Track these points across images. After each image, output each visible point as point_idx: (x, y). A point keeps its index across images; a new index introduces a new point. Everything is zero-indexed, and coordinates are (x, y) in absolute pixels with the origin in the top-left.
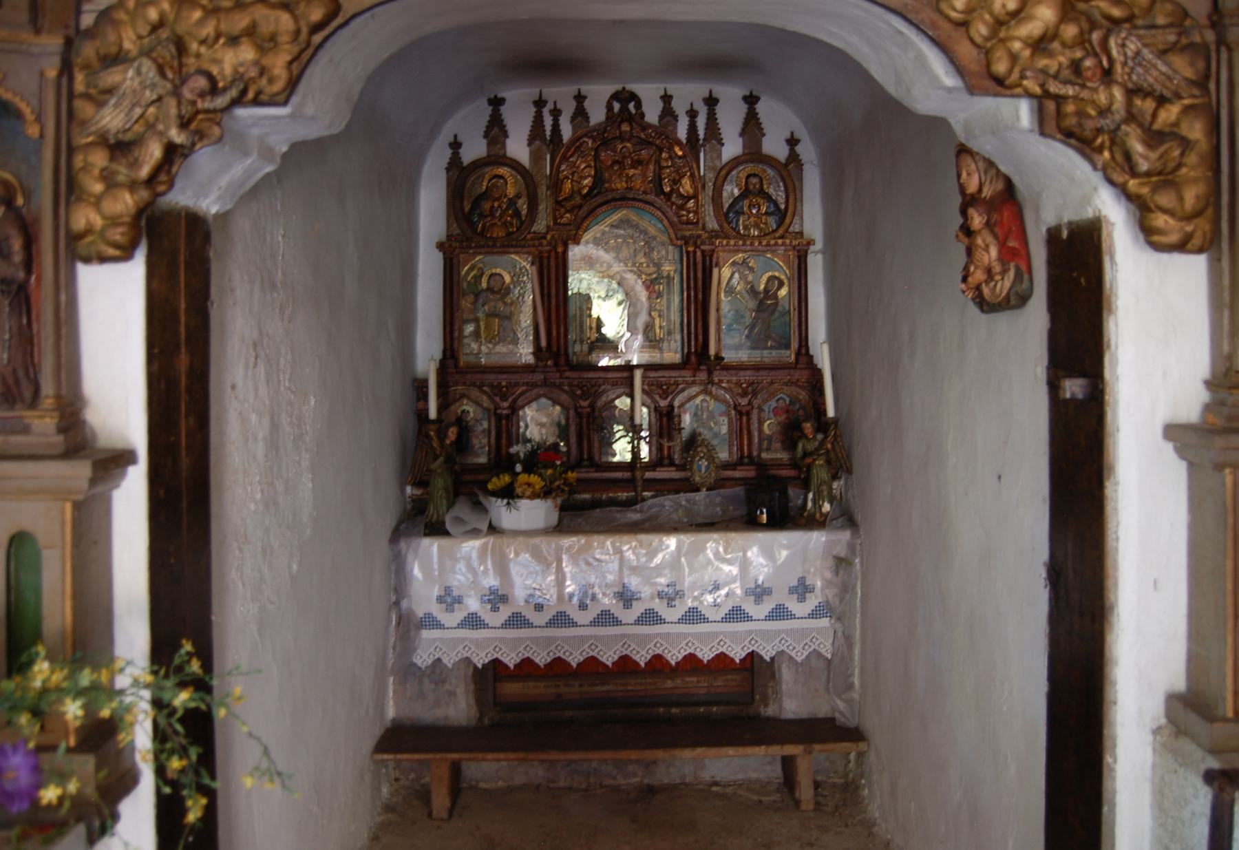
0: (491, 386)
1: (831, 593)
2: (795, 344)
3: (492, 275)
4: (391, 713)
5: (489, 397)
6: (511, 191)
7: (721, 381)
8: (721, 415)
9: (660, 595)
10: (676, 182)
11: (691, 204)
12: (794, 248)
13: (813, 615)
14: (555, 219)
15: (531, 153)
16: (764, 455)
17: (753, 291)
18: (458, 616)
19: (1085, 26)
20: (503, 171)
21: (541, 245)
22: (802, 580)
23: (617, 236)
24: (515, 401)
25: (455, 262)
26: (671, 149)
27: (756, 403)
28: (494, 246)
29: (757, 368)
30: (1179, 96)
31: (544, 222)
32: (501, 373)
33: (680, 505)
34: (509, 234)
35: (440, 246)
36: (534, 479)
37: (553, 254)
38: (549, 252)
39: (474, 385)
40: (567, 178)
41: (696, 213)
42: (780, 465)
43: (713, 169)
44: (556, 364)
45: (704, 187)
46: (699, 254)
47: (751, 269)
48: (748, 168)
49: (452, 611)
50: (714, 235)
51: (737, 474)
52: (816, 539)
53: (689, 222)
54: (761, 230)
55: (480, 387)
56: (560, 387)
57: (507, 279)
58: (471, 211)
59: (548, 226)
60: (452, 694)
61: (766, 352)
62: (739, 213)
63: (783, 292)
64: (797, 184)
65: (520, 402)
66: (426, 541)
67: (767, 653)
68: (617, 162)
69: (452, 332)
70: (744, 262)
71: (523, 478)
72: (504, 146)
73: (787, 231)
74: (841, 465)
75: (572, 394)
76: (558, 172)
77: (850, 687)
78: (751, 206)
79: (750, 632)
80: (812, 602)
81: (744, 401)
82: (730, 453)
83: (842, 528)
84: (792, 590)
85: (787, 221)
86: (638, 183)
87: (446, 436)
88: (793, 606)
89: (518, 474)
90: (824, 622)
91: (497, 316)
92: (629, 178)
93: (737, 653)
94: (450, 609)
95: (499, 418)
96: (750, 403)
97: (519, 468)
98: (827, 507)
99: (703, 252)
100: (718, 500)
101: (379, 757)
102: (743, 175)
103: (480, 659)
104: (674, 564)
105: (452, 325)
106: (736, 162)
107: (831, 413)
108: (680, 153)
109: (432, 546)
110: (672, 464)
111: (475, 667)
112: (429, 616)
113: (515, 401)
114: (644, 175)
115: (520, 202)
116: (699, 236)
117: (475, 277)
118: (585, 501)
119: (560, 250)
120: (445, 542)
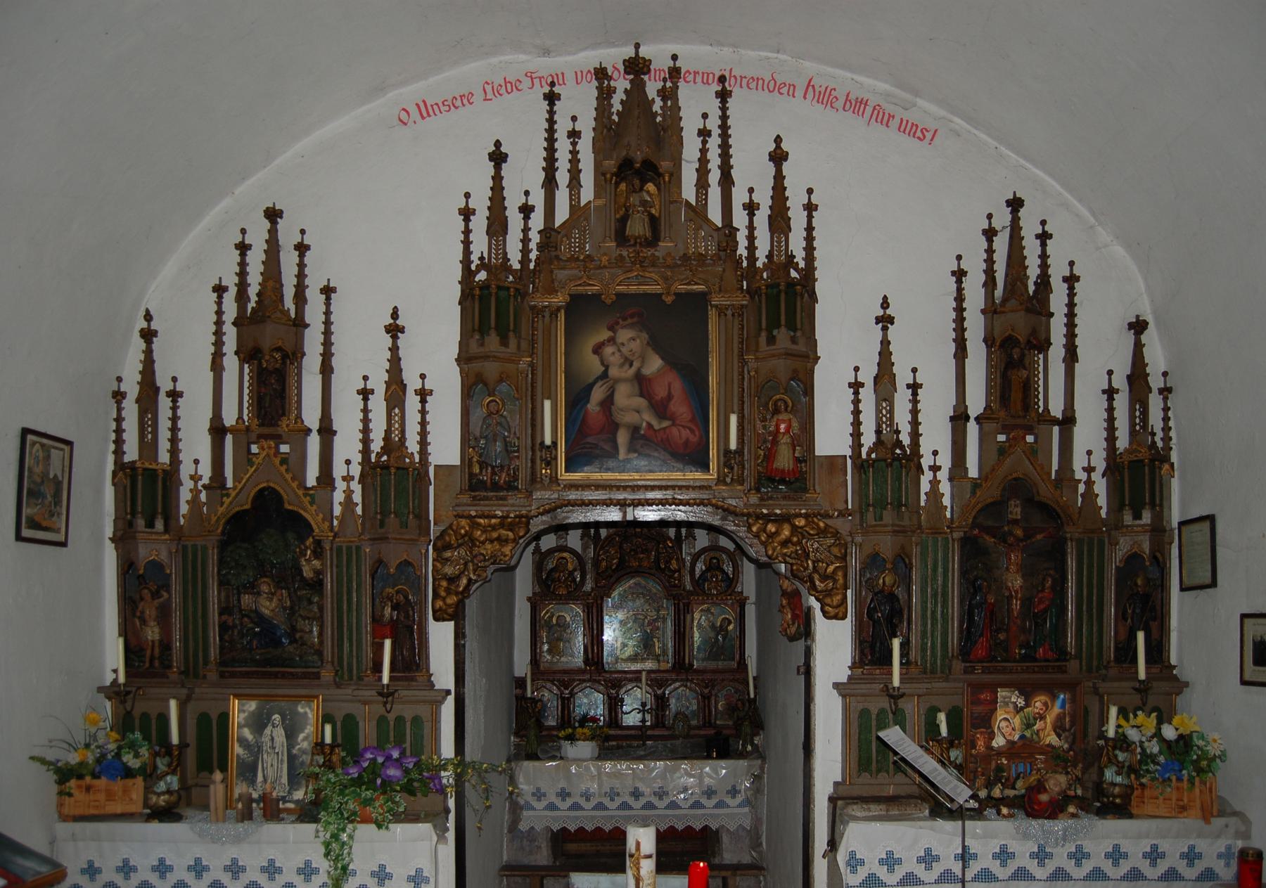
0: (558, 681)
1: (749, 793)
2: (737, 657)
3: (559, 616)
4: (505, 858)
5: (557, 687)
6: (570, 567)
7: (693, 679)
8: (693, 699)
9: (655, 793)
10: (668, 562)
11: (676, 575)
12: (737, 601)
13: (739, 806)
14: (596, 585)
15: (582, 544)
16: (718, 722)
17: (713, 627)
18: (544, 803)
19: (800, 537)
20: (565, 555)
21: (588, 599)
22: (734, 787)
23: (633, 593)
24: (572, 690)
25: (538, 608)
26: (665, 541)
27: (713, 693)
28: (561, 599)
29: (714, 671)
30: (832, 563)
31: (590, 585)
32: (565, 673)
33: (667, 747)
34: (569, 592)
35: (529, 599)
36: (585, 730)
37: (595, 605)
38: (593, 603)
39: (549, 680)
40: (603, 559)
41: (679, 580)
42: (727, 727)
43: (690, 554)
44: (597, 669)
45: (684, 566)
46: (681, 604)
47: (712, 613)
48: (712, 554)
49: (540, 801)
50: (690, 593)
51: (702, 732)
52: (743, 764)
53: (675, 586)
54: (717, 590)
55: (552, 682)
56: (599, 682)
57: (568, 619)
58: (547, 577)
59: (592, 588)
60: (540, 847)
61: (720, 663)
62: (705, 580)
63: (731, 627)
64: (740, 563)
65: (575, 691)
66: (526, 763)
67: (714, 826)
68: (634, 550)
69: (536, 649)
70: (708, 610)
71: (579, 730)
72: (566, 540)
73: (733, 591)
74: (758, 725)
75: (606, 687)
76: (599, 555)
77: (761, 844)
78: (712, 578)
79: (704, 815)
80: (739, 798)
81: (706, 691)
82: (698, 721)
83: (757, 758)
84: (728, 792)
85: (734, 585)
86: (645, 564)
87: (536, 707)
88: (729, 800)
89: (576, 728)
90: (746, 810)
91: (561, 640)
92: (640, 560)
93: (698, 826)
94: (539, 800)
95: (563, 699)
96: (710, 692)
97: (577, 724)
98: (749, 748)
99: (684, 603)
100: (689, 745)
101: (503, 873)
102: (708, 558)
103: (556, 827)
104: (663, 776)
105: (536, 645)
106: (704, 550)
107: (752, 696)
108: (670, 545)
109: (529, 765)
110: (664, 726)
111: (552, 830)
112: (527, 803)
113: (572, 690)
114: (649, 557)
115: (576, 573)
116: (681, 594)
117: (549, 617)
118: (613, 746)
119: (599, 602)
120: (537, 764)
